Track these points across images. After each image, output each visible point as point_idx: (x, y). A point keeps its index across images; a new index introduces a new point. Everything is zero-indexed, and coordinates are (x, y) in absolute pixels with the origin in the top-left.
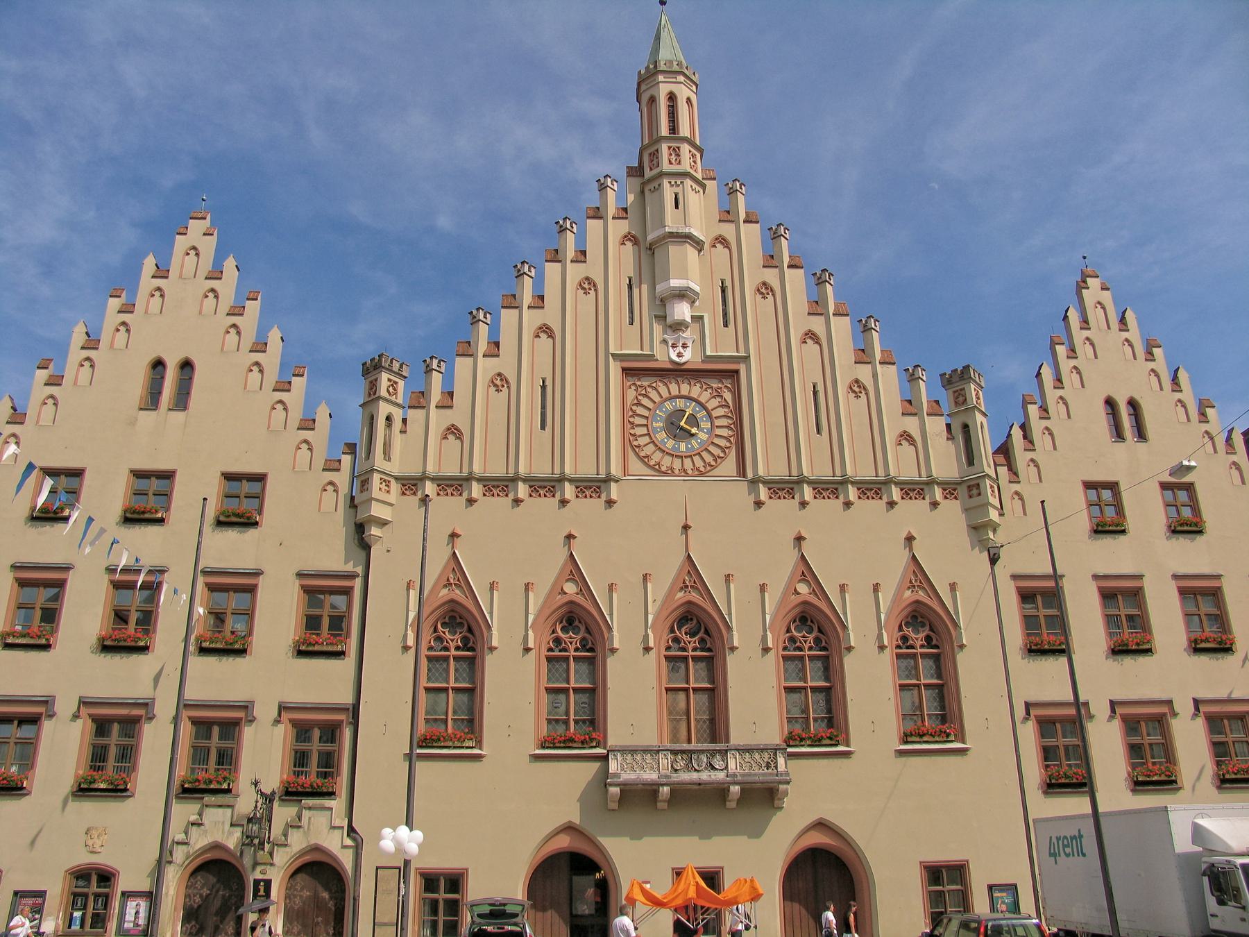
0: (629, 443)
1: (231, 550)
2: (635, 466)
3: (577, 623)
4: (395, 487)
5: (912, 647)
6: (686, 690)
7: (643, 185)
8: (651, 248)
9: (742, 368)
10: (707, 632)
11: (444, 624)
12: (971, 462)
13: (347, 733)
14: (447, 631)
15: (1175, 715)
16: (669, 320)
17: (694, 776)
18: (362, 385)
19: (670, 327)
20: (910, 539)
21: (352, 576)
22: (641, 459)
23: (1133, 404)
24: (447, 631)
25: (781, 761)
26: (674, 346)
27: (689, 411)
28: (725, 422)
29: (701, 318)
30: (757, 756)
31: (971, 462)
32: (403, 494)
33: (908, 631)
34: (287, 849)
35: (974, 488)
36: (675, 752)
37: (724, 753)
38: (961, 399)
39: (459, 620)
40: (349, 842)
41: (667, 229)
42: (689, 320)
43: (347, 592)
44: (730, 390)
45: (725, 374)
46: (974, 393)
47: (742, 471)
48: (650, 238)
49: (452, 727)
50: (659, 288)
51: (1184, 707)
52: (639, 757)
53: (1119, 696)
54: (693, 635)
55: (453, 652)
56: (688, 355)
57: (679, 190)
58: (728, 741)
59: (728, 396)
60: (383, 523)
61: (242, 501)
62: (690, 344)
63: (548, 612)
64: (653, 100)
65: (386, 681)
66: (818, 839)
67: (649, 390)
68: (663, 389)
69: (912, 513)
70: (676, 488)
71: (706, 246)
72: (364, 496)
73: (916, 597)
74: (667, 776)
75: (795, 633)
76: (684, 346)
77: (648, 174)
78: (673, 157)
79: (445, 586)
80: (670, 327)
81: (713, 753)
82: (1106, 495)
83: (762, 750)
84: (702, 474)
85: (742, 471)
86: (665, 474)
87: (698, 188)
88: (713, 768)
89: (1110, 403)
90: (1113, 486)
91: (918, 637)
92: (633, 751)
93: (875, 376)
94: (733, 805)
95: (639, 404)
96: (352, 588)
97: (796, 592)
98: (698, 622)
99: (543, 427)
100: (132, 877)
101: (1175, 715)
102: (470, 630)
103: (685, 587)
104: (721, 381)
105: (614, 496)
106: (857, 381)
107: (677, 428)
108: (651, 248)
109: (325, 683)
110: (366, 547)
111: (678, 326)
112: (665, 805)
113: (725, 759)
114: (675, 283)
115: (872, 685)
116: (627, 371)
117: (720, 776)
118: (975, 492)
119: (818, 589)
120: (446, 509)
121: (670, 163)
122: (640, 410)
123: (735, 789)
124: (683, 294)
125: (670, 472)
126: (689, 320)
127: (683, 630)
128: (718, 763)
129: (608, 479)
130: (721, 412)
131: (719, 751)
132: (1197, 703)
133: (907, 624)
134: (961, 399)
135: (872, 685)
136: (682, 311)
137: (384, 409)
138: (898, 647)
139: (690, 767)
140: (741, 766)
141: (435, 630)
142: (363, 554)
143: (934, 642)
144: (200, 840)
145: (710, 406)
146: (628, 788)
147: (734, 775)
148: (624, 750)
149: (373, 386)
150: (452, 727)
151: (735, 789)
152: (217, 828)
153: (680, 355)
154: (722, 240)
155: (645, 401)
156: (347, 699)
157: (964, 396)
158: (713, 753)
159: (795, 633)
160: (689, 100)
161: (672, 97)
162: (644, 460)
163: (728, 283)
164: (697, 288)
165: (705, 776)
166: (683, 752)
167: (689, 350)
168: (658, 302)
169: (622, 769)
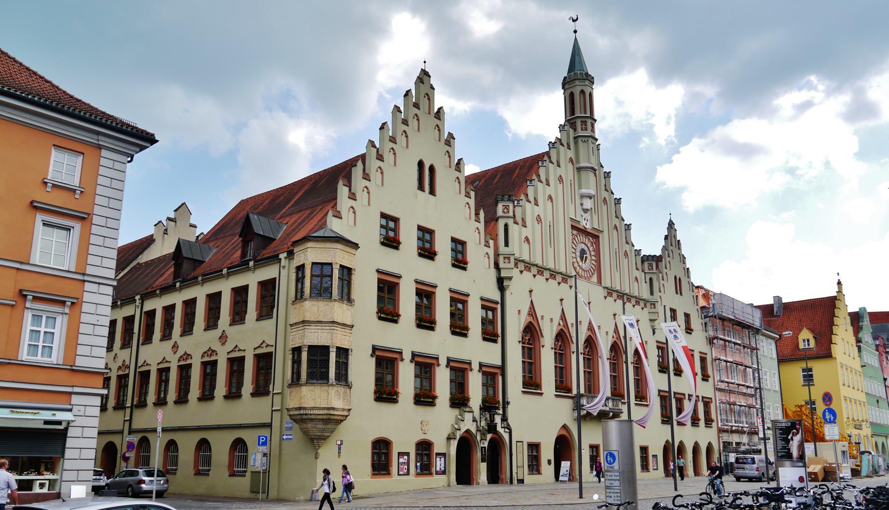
9: (601, 236)
12: (652, 294)
21: (497, 303)
35: (653, 305)
43: (494, 310)
47: (600, 281)
48: (582, 165)
72: (507, 265)
85: (600, 281)
89: (675, 277)
96: (496, 309)
100: (439, 446)
108: (579, 169)
109: (490, 354)
111: (586, 211)
116: (573, 227)
152: (468, 424)
156: (499, 363)
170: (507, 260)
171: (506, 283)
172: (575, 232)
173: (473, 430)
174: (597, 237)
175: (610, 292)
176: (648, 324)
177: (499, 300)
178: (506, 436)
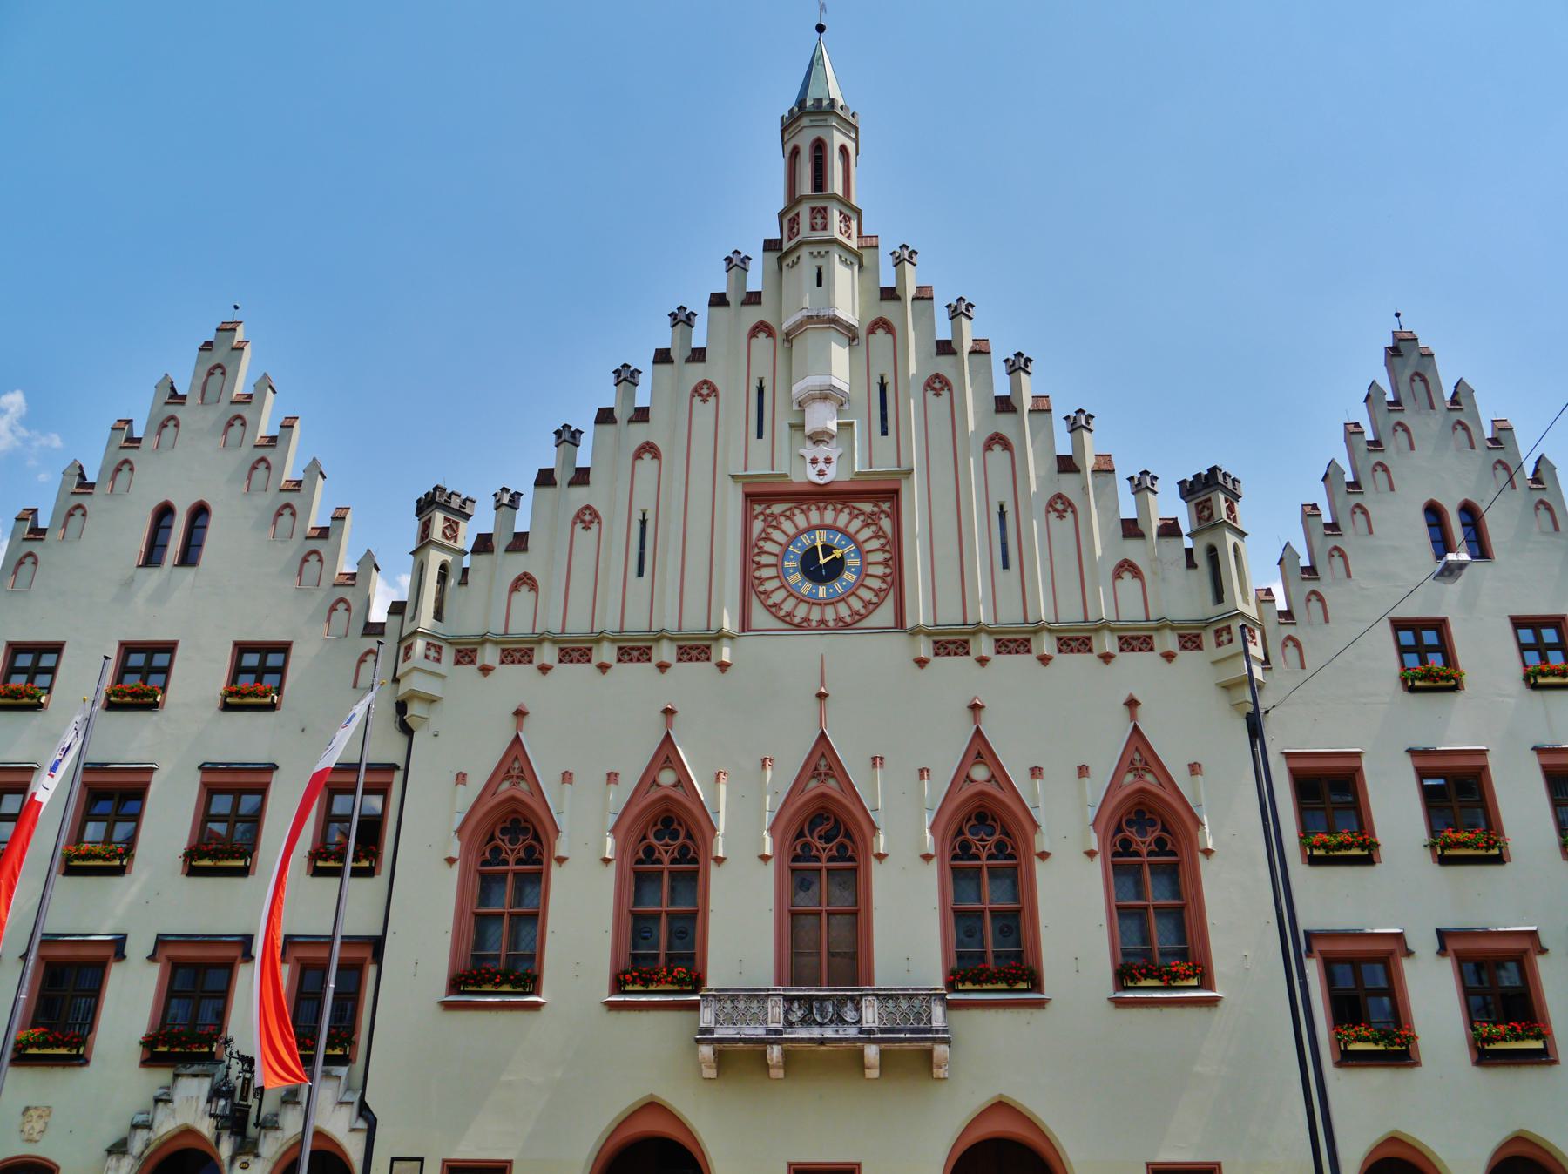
0: (749, 586)
1: (245, 739)
2: (760, 617)
3: (675, 826)
4: (448, 654)
5: (1137, 854)
6: (819, 914)
7: (780, 260)
8: (789, 338)
10: (848, 835)
11: (504, 831)
12: (1219, 596)
13: (371, 971)
14: (506, 838)
15: (1409, 953)
16: (808, 430)
17: (816, 1033)
18: (415, 525)
19: (810, 437)
20: (1132, 704)
21: (394, 767)
22: (768, 608)
23: (1470, 513)
24: (506, 838)
25: (938, 1011)
26: (814, 461)
27: (819, 544)
28: (880, 557)
29: (851, 424)
30: (904, 1004)
31: (1219, 596)
32: (458, 662)
33: (1131, 833)
34: (279, 1134)
36: (789, 999)
37: (856, 1002)
38: (1206, 513)
39: (523, 824)
40: (362, 1124)
41: (805, 313)
42: (832, 426)
44: (888, 516)
45: (884, 494)
46: (1224, 506)
47: (900, 621)
48: (785, 326)
49: (498, 968)
50: (796, 388)
51: (1423, 942)
52: (741, 1005)
53: (1450, 923)
54: (828, 838)
55: (512, 867)
56: (832, 474)
57: (819, 262)
58: (870, 981)
59: (886, 524)
60: (431, 700)
61: (257, 675)
62: (834, 459)
63: (635, 810)
64: (795, 152)
65: (420, 905)
66: (1000, 1126)
67: (782, 519)
68: (800, 520)
69: (1137, 671)
70: (810, 645)
71: (862, 333)
73: (1140, 784)
74: (777, 1032)
75: (969, 836)
76: (828, 461)
77: (786, 246)
78: (819, 221)
79: (505, 779)
80: (810, 437)
81: (841, 1001)
82: (1430, 638)
83: (911, 997)
84: (848, 626)
85: (900, 621)
86: (799, 627)
87: (850, 259)
88: (843, 1021)
90: (1440, 625)
91: (1143, 842)
92: (734, 998)
93: (1085, 489)
94: (873, 1073)
95: (768, 539)
96: (389, 785)
97: (969, 778)
98: (836, 821)
99: (640, 573)
101: (1409, 953)
102: (537, 837)
103: (816, 774)
104: (876, 505)
105: (726, 657)
106: (1060, 496)
107: (820, 568)
108: (789, 338)
110: (407, 730)
111: (818, 438)
112: (780, 1073)
113: (858, 1009)
114: (813, 381)
115: (1072, 907)
116: (752, 498)
117: (852, 1032)
118: (1225, 637)
119: (999, 775)
120: (515, 681)
121: (813, 228)
122: (769, 546)
123: (872, 1052)
124: (826, 395)
125: (802, 626)
126: (832, 426)
127: (815, 835)
128: (850, 1015)
129: (720, 636)
130: (875, 544)
131: (852, 998)
132: (1442, 935)
133: (1130, 823)
134: (1206, 513)
135: (1072, 907)
136: (823, 418)
137: (435, 558)
138: (1115, 854)
139: (807, 1021)
140: (881, 1019)
141: (492, 838)
142: (405, 740)
143: (1169, 847)
144: (166, 1124)
145: (862, 536)
146: (727, 1047)
147: (870, 1031)
148: (719, 996)
149: (426, 528)
150: (498, 968)
151: (872, 1052)
153: (821, 473)
154: (881, 324)
155: (776, 535)
157: (1210, 508)
158: (841, 1001)
159: (969, 836)
160: (843, 149)
161: (819, 147)
162: (773, 609)
163: (889, 379)
164: (846, 388)
165: (829, 1033)
166: (799, 998)
167: (833, 467)
168: (796, 408)
169: (717, 1022)
170: (432, 653)
171: (414, 709)
172: (777, 509)
173: (206, 1127)
174: (893, 495)
175: (952, 644)
176: (1220, 702)
177: (402, 765)
178: (353, 1148)
